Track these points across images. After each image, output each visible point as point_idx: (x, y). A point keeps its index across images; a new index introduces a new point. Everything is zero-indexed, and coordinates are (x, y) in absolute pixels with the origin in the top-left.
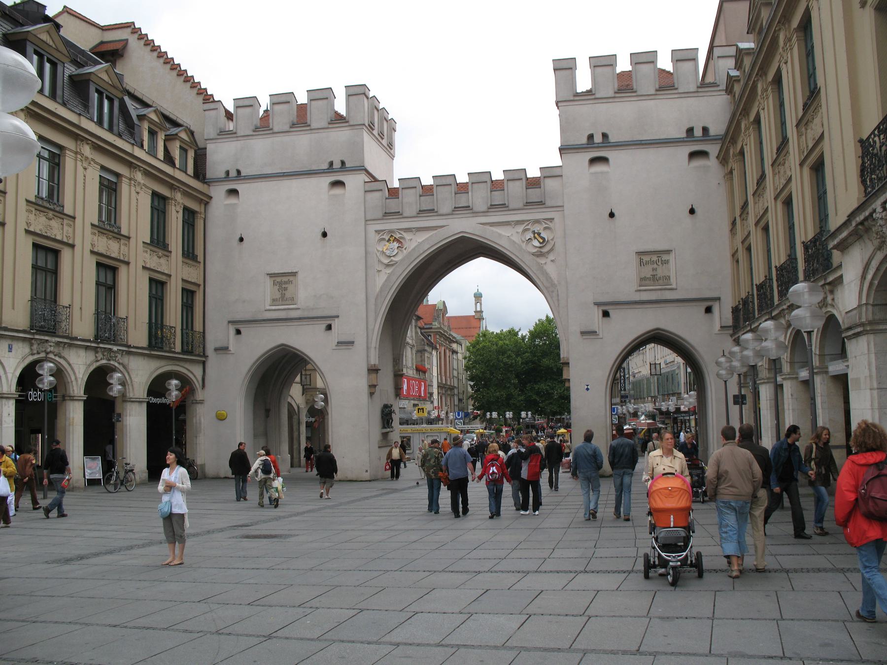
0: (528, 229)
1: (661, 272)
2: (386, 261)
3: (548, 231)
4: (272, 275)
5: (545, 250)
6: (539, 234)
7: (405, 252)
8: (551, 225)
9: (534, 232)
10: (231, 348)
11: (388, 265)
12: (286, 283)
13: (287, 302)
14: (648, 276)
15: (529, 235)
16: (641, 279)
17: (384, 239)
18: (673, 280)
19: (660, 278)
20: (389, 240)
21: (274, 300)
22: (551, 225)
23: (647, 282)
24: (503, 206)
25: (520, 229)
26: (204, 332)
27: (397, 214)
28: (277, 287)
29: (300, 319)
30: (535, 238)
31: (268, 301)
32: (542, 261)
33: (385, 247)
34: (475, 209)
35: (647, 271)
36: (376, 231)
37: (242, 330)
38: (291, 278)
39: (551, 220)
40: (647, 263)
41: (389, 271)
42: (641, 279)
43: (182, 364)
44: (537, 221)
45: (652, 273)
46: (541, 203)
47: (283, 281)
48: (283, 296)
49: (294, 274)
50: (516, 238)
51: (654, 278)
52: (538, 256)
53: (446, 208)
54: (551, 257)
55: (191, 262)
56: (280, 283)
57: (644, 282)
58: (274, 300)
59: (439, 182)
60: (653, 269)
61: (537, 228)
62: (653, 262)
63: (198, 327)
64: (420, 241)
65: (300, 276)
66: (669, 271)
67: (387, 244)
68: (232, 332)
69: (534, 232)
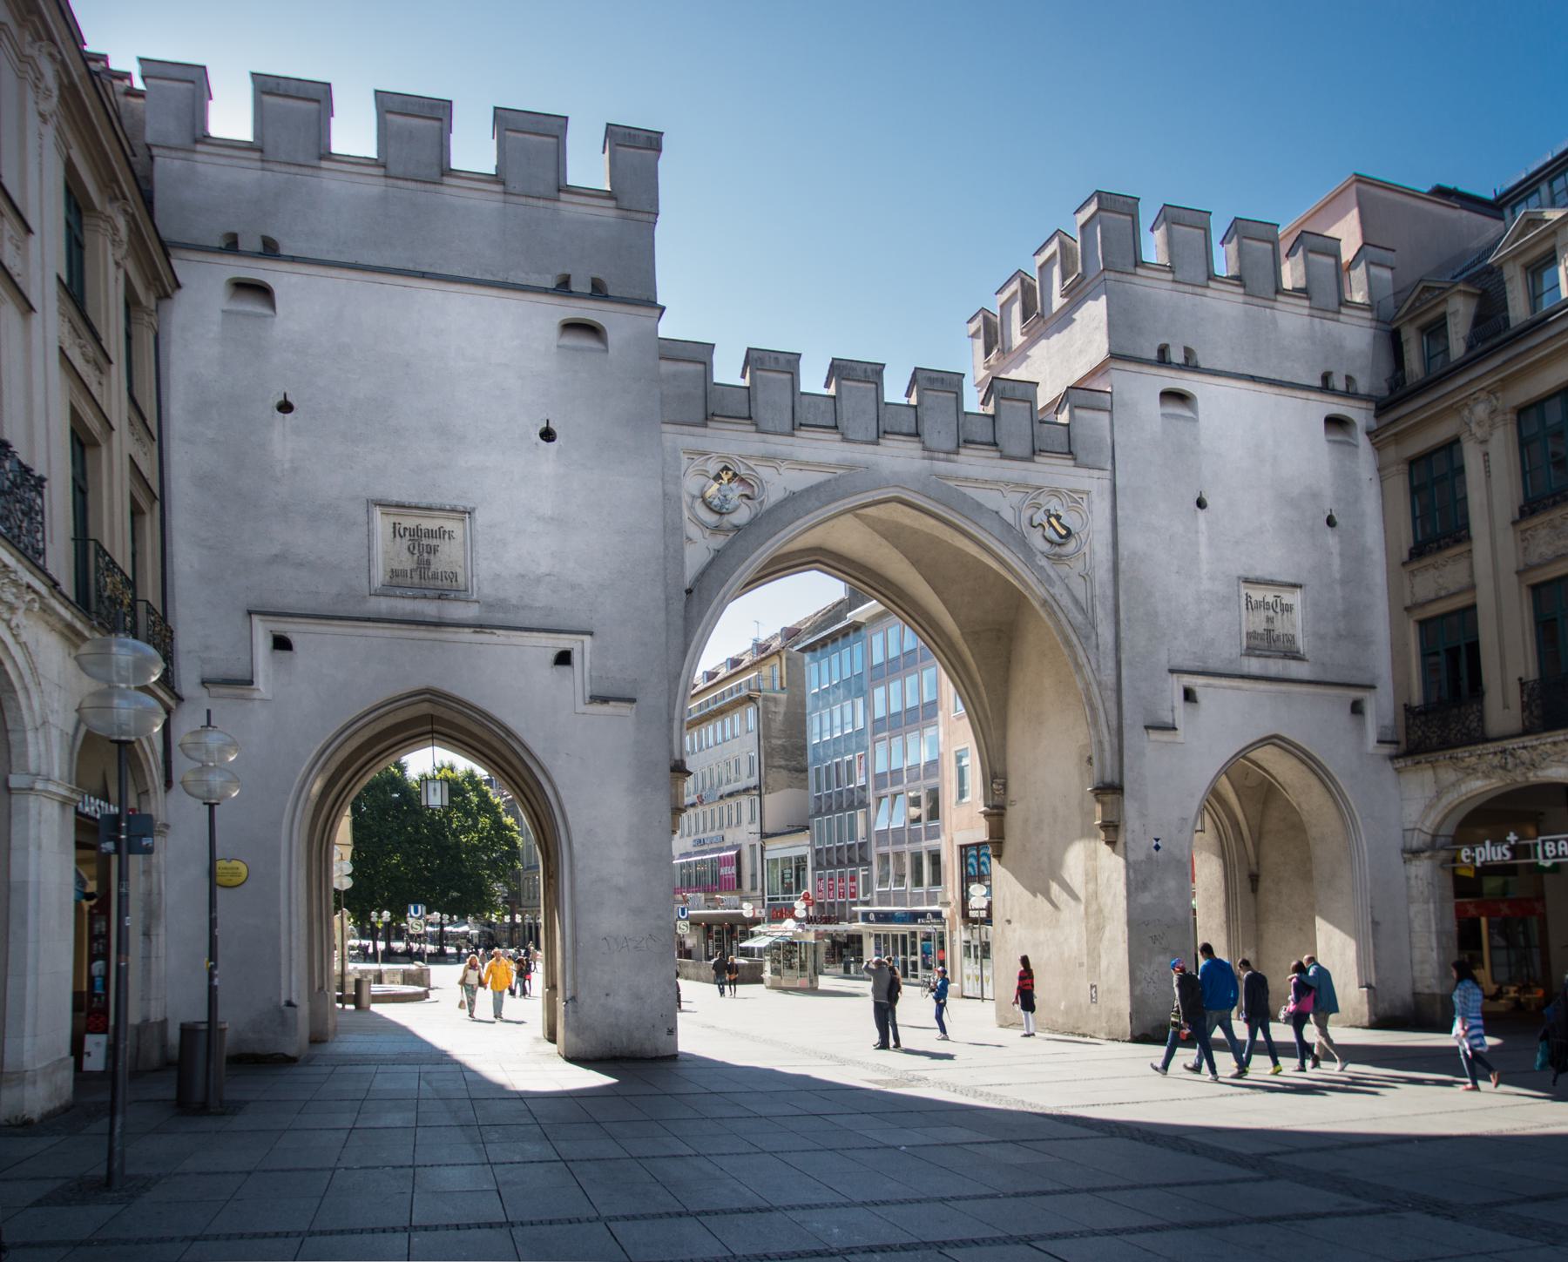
1: (1281, 626)
5: (1071, 546)
21: (394, 573)
28: (406, 542)
31: (379, 576)
35: (1257, 622)
48: (423, 565)
56: (416, 534)
58: (394, 573)
60: (1269, 620)
66: (1293, 626)
68: (262, 644)
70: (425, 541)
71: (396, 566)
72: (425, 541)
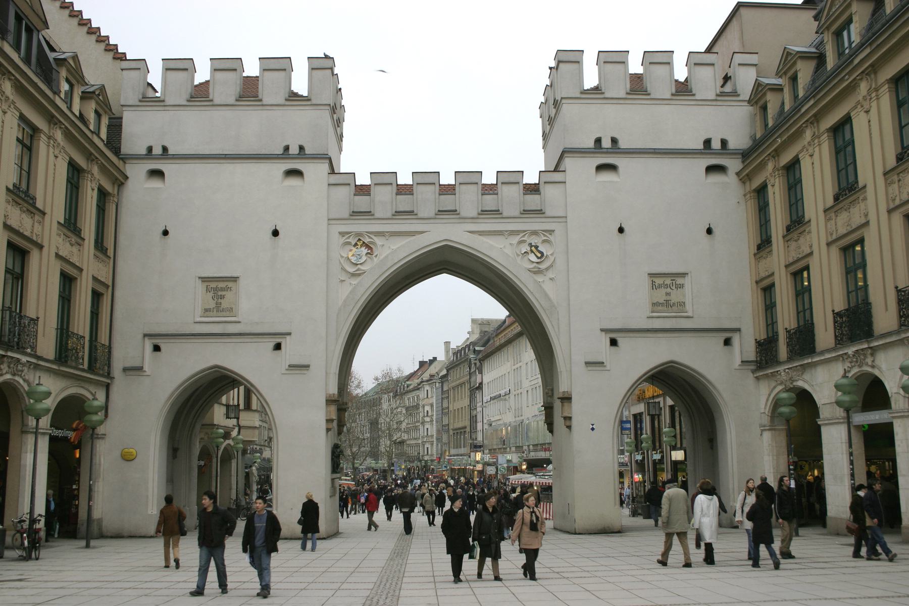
0: (524, 241)
1: (675, 297)
2: (352, 269)
3: (547, 245)
4: (204, 279)
5: (543, 266)
6: (536, 247)
7: (375, 259)
8: (551, 238)
9: (531, 245)
10: (146, 368)
11: (353, 275)
12: (222, 289)
13: (224, 314)
14: (661, 301)
15: (525, 248)
16: (654, 304)
17: (349, 243)
18: (688, 307)
19: (674, 304)
20: (356, 245)
21: (206, 310)
22: (551, 238)
23: (660, 308)
24: (496, 212)
25: (515, 240)
26: (110, 347)
27: (367, 214)
28: (211, 294)
29: (240, 334)
30: (532, 251)
31: (199, 311)
32: (539, 278)
33: (351, 253)
34: (463, 214)
36: (340, 233)
37: (162, 347)
38: (230, 284)
39: (551, 232)
40: (660, 286)
41: (354, 281)
42: (654, 304)
43: (83, 384)
44: (535, 233)
45: (665, 298)
46: (540, 212)
47: (219, 287)
48: (218, 305)
49: (235, 279)
50: (508, 251)
51: (667, 304)
52: (535, 273)
53: (427, 210)
54: (550, 274)
55: (101, 256)
56: (216, 289)
57: (656, 308)
59: (420, 179)
60: (668, 294)
61: (535, 240)
62: (666, 286)
63: (103, 338)
64: (394, 248)
65: (242, 282)
66: (684, 296)
67: (354, 249)
68: (149, 347)
69: (531, 245)
70: (220, 293)
71: (207, 307)
72: (220, 293)
